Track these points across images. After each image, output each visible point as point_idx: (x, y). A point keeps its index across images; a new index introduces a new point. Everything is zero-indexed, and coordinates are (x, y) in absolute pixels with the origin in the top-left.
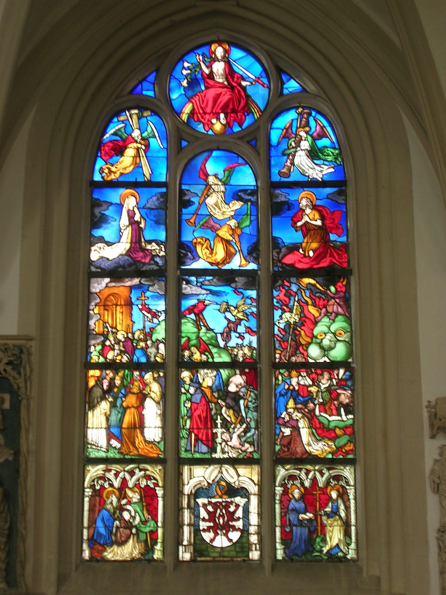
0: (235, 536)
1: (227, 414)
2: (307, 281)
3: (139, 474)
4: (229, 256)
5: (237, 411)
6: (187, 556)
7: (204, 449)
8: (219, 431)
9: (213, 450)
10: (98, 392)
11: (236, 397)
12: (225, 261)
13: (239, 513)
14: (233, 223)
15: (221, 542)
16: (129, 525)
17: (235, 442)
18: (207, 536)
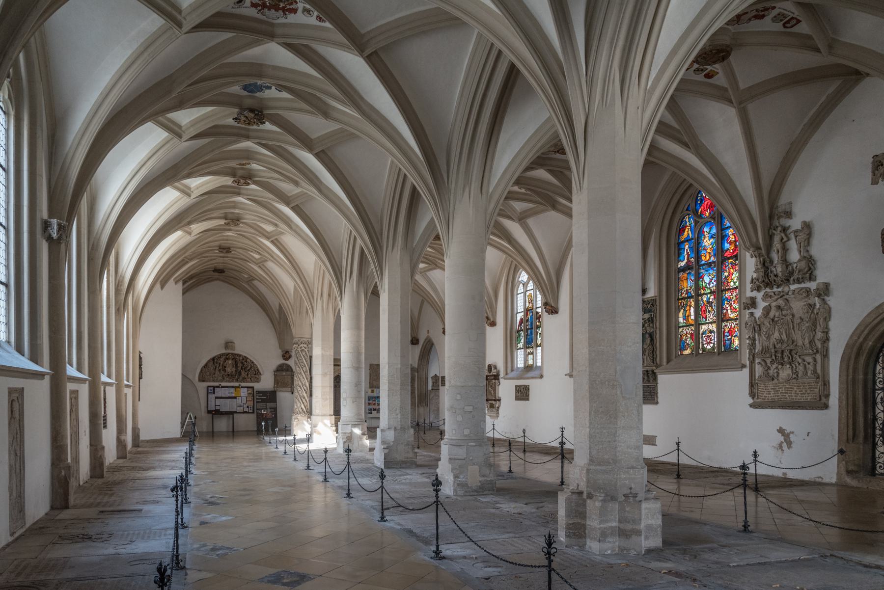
0: (712, 345)
1: (710, 308)
2: (730, 261)
3: (690, 329)
4: (710, 257)
5: (712, 307)
6: (701, 352)
7: (704, 320)
8: (707, 314)
9: (706, 320)
10: (680, 307)
11: (712, 303)
12: (709, 260)
13: (713, 338)
14: (711, 246)
15: (709, 347)
16: (688, 344)
17: (711, 317)
18: (705, 346)
